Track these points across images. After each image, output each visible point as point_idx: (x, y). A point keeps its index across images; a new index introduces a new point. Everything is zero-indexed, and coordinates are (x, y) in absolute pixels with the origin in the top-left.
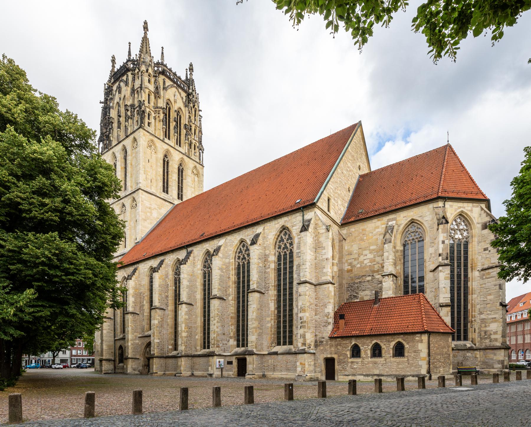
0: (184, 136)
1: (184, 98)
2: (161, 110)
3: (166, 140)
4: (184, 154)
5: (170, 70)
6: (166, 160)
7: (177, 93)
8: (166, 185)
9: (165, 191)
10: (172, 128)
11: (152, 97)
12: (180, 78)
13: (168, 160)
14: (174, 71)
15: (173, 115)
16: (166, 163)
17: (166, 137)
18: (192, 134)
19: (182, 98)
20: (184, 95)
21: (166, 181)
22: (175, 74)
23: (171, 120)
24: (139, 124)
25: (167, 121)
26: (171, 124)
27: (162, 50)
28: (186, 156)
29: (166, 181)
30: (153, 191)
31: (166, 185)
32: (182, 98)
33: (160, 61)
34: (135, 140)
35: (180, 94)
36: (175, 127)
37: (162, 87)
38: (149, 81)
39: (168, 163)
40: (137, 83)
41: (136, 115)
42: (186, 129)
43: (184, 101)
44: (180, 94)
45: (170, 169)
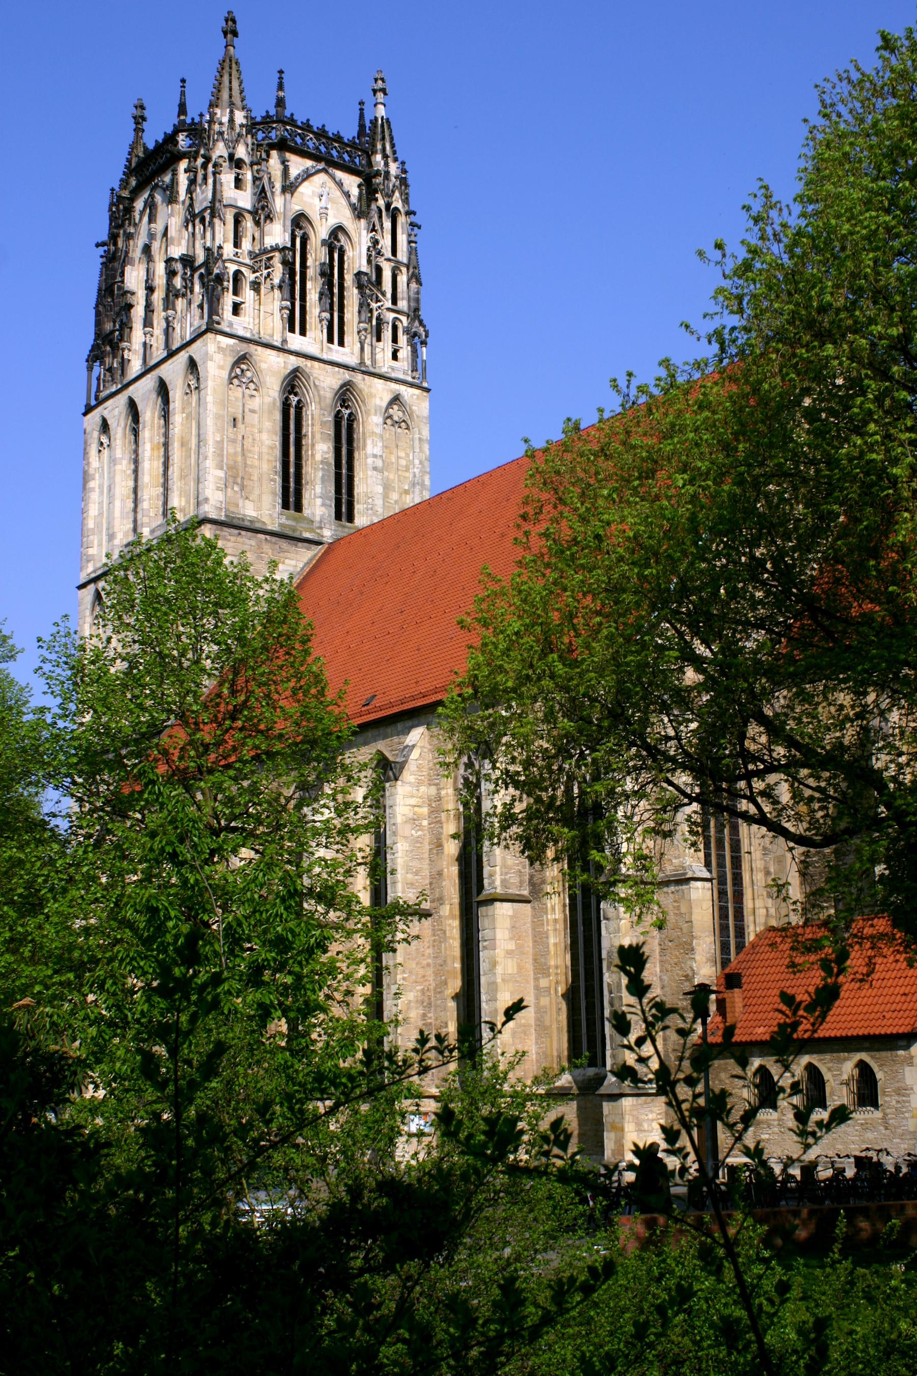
0: (356, 309)
1: (355, 192)
2: (277, 254)
3: (296, 341)
4: (353, 369)
5: (307, 127)
6: (294, 404)
7: (331, 184)
8: (292, 485)
9: (292, 505)
10: (313, 296)
11: (248, 224)
12: (338, 138)
13: (299, 402)
14: (316, 124)
15: (317, 256)
16: (292, 411)
17: (292, 330)
18: (384, 294)
19: (347, 195)
20: (352, 183)
21: (292, 470)
22: (321, 134)
23: (310, 272)
24: (206, 316)
25: (298, 278)
26: (309, 285)
27: (281, 78)
28: (364, 372)
29: (292, 470)
30: (249, 511)
31: (292, 485)
32: (347, 195)
33: (272, 112)
34: (192, 365)
35: (340, 184)
36: (321, 294)
37: (278, 186)
38: (239, 183)
39: (299, 408)
40: (203, 196)
41: (197, 288)
42: (360, 287)
43: (354, 200)
44: (340, 184)
45: (307, 429)
